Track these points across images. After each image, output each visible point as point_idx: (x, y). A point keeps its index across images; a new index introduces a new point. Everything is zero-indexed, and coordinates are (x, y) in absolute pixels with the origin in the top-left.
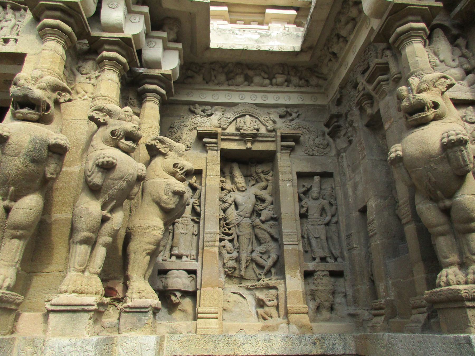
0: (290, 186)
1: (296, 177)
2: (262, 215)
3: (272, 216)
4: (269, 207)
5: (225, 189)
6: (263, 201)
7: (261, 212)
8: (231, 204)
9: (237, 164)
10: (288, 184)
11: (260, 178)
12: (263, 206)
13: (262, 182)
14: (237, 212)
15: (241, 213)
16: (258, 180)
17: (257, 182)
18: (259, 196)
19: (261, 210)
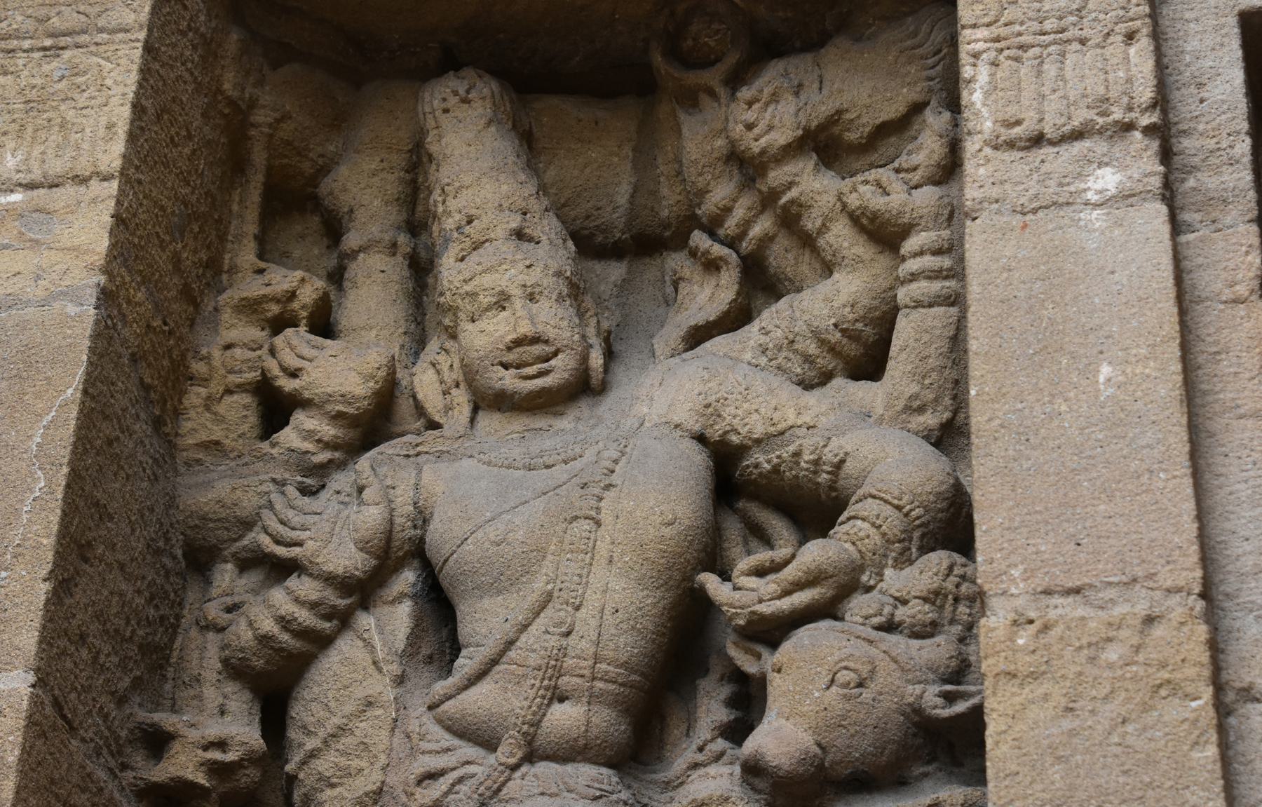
0: (1125, 197)
1: (1237, 76)
2: (777, 686)
3: (931, 698)
4: (895, 580)
5: (296, 402)
6: (815, 506)
7: (770, 659)
8: (362, 591)
9: (487, 88)
10: (1107, 180)
11: (790, 220)
12: (790, 573)
13: (828, 269)
14: (441, 687)
15: (482, 700)
16: (782, 257)
17: (761, 283)
18: (761, 460)
19: (769, 632)
